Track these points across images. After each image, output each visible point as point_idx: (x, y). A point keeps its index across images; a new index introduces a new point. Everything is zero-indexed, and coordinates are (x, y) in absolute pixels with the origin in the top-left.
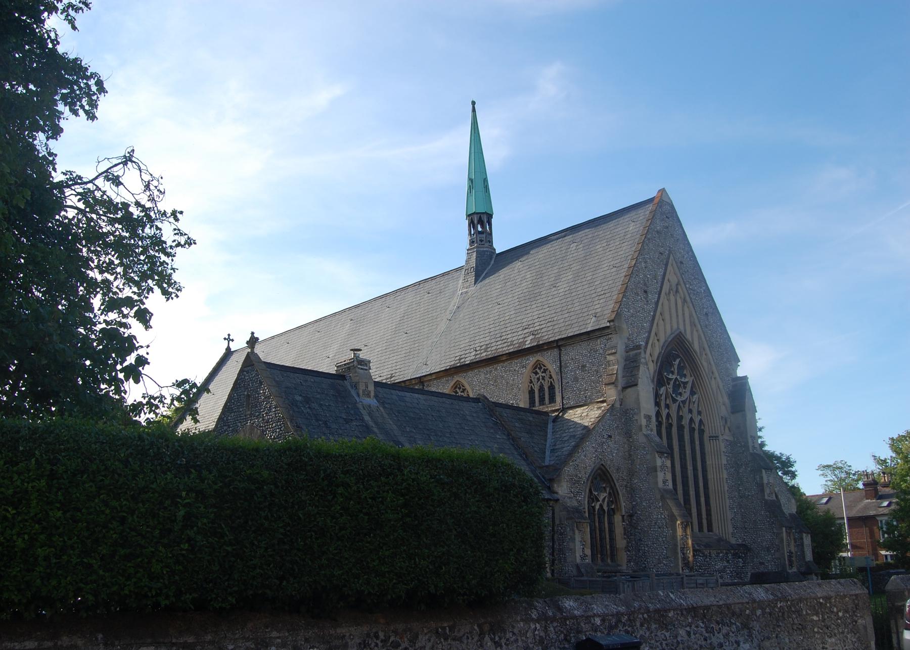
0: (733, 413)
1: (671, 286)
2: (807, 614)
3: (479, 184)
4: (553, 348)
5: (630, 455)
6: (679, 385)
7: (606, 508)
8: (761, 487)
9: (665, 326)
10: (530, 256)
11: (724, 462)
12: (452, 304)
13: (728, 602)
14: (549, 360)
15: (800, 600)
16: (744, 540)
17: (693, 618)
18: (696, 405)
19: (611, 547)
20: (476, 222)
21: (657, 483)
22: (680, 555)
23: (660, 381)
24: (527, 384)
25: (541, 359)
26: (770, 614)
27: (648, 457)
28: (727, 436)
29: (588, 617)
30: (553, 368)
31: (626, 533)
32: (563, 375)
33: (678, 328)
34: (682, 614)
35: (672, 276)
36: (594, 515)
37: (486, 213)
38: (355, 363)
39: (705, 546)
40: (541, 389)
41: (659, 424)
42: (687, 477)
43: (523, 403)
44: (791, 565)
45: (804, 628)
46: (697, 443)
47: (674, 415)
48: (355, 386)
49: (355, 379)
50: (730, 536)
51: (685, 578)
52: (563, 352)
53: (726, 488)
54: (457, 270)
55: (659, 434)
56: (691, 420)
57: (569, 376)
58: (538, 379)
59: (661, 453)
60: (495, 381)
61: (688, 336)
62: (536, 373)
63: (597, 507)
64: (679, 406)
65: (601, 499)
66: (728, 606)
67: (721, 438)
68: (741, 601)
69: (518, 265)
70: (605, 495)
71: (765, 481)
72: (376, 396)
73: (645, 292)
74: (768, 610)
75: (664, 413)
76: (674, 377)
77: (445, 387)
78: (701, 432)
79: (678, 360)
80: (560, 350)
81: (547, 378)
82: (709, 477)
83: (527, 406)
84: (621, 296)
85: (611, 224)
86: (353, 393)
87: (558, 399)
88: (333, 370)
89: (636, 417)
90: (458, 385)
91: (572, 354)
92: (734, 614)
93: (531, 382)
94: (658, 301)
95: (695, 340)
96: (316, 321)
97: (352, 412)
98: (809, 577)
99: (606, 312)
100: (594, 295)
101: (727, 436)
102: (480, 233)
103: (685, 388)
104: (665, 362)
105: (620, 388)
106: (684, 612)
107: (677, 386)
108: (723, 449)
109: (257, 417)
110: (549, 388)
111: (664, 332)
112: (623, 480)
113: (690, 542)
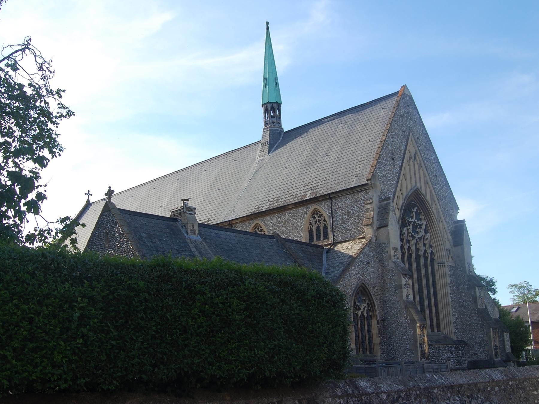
0: (454, 246)
1: (410, 155)
2: (530, 390)
3: (271, 82)
4: (326, 199)
5: (383, 276)
6: (417, 226)
7: (365, 315)
8: (475, 299)
9: (406, 183)
10: (309, 134)
11: (449, 281)
12: (252, 168)
13: (475, 381)
14: (323, 208)
15: (525, 380)
16: (463, 338)
17: (451, 393)
18: (428, 240)
19: (369, 343)
20: (269, 109)
21: (402, 297)
22: (419, 349)
23: (403, 224)
24: (307, 225)
25: (317, 207)
26: (504, 390)
27: (396, 278)
28: (451, 263)
29: (377, 394)
30: (326, 214)
31: (381, 333)
32: (334, 219)
33: (416, 186)
34: (444, 391)
35: (411, 148)
36: (357, 320)
37: (276, 103)
38: (185, 210)
39: (435, 342)
40: (318, 229)
41: (403, 254)
42: (423, 293)
43: (305, 239)
44: (496, 355)
45: (528, 400)
46: (429, 268)
48: (185, 227)
49: (185, 221)
50: (453, 334)
51: (425, 365)
52: (334, 202)
53: (450, 300)
54: (255, 144)
55: (403, 261)
56: (425, 251)
57: (338, 219)
58: (316, 222)
59: (405, 275)
60: (284, 224)
61: (423, 192)
62: (314, 218)
63: (360, 314)
65: (362, 308)
66: (475, 385)
67: (446, 264)
68: (484, 380)
69: (299, 140)
70: (365, 305)
71: (478, 295)
72: (200, 234)
73: (393, 159)
74: (503, 387)
75: (406, 246)
76: (413, 220)
77: (249, 227)
78: (432, 260)
79: (416, 209)
80: (332, 201)
81: (322, 221)
83: (308, 241)
84: (376, 162)
85: (368, 111)
86: (183, 231)
87: (330, 236)
88: (168, 215)
89: (387, 249)
90: (257, 227)
91: (340, 204)
92: (479, 390)
93: (310, 224)
94: (402, 166)
96: (153, 181)
97: (183, 245)
98: (508, 363)
99: (364, 174)
100: (356, 161)
101: (451, 263)
102: (272, 117)
103: (421, 228)
104: (407, 210)
105: (375, 228)
106: (445, 390)
107: (415, 227)
108: (448, 272)
109: (113, 249)
110: (324, 228)
111: (406, 188)
112: (378, 294)
113: (426, 339)
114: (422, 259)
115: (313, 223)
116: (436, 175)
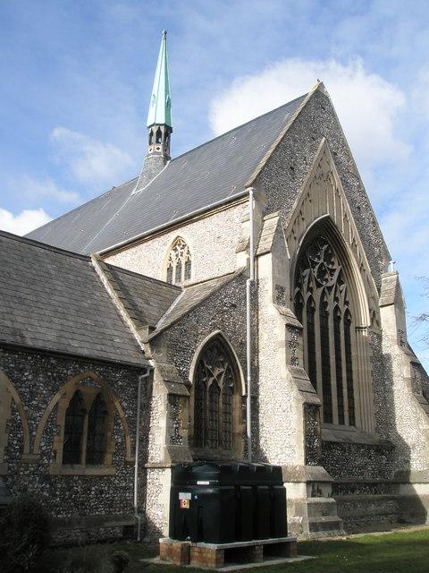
6: (325, 272)
7: (221, 384)
40: (179, 267)
46: (342, 332)
47: (317, 298)
56: (337, 309)
58: (177, 255)
62: (175, 250)
63: (210, 383)
64: (324, 291)
65: (216, 373)
70: (222, 370)
75: (306, 296)
78: (348, 323)
81: (185, 254)
82: (354, 368)
95: (349, 233)
103: (332, 275)
107: (322, 273)
114: (331, 318)
115: (174, 257)
116: (359, 208)
